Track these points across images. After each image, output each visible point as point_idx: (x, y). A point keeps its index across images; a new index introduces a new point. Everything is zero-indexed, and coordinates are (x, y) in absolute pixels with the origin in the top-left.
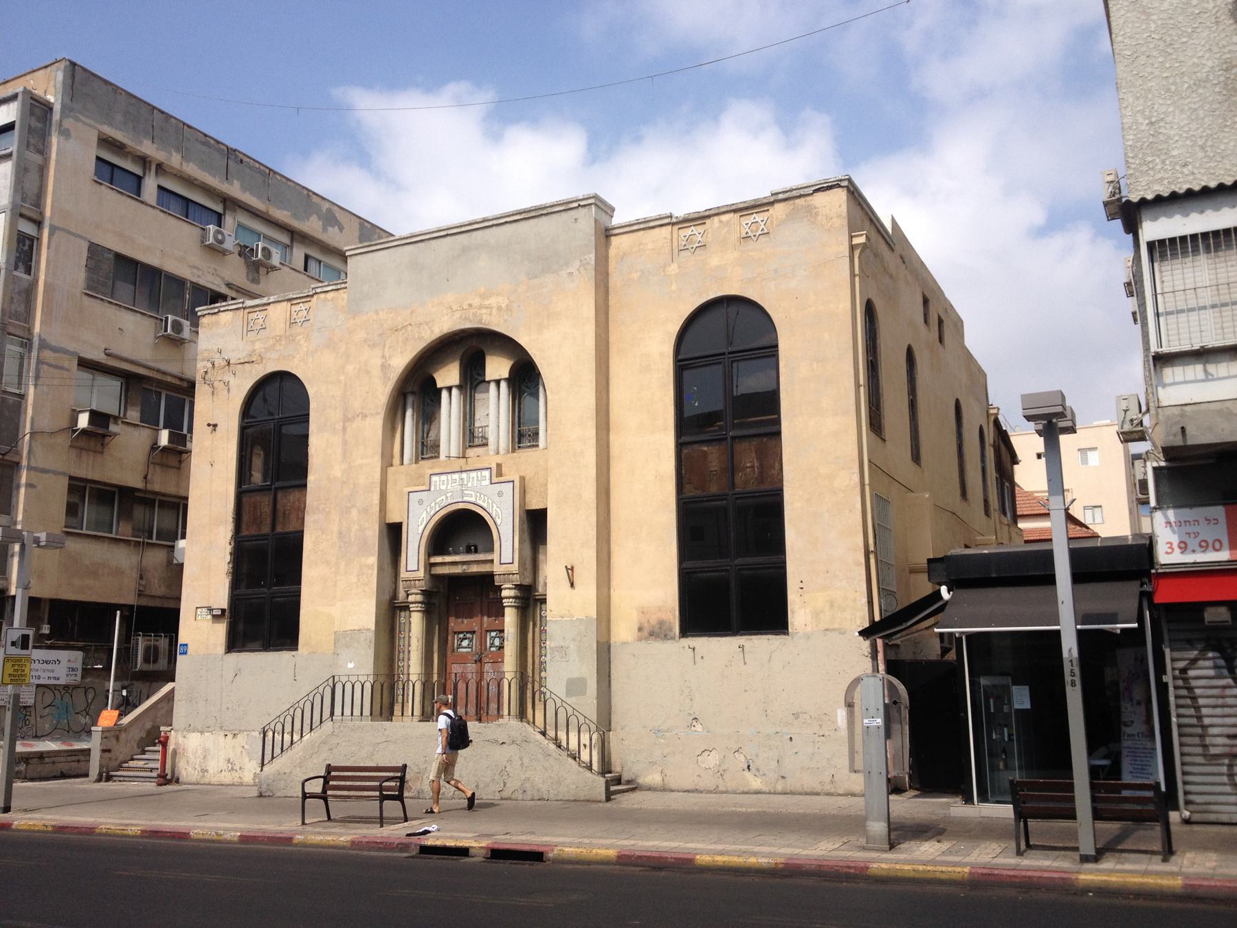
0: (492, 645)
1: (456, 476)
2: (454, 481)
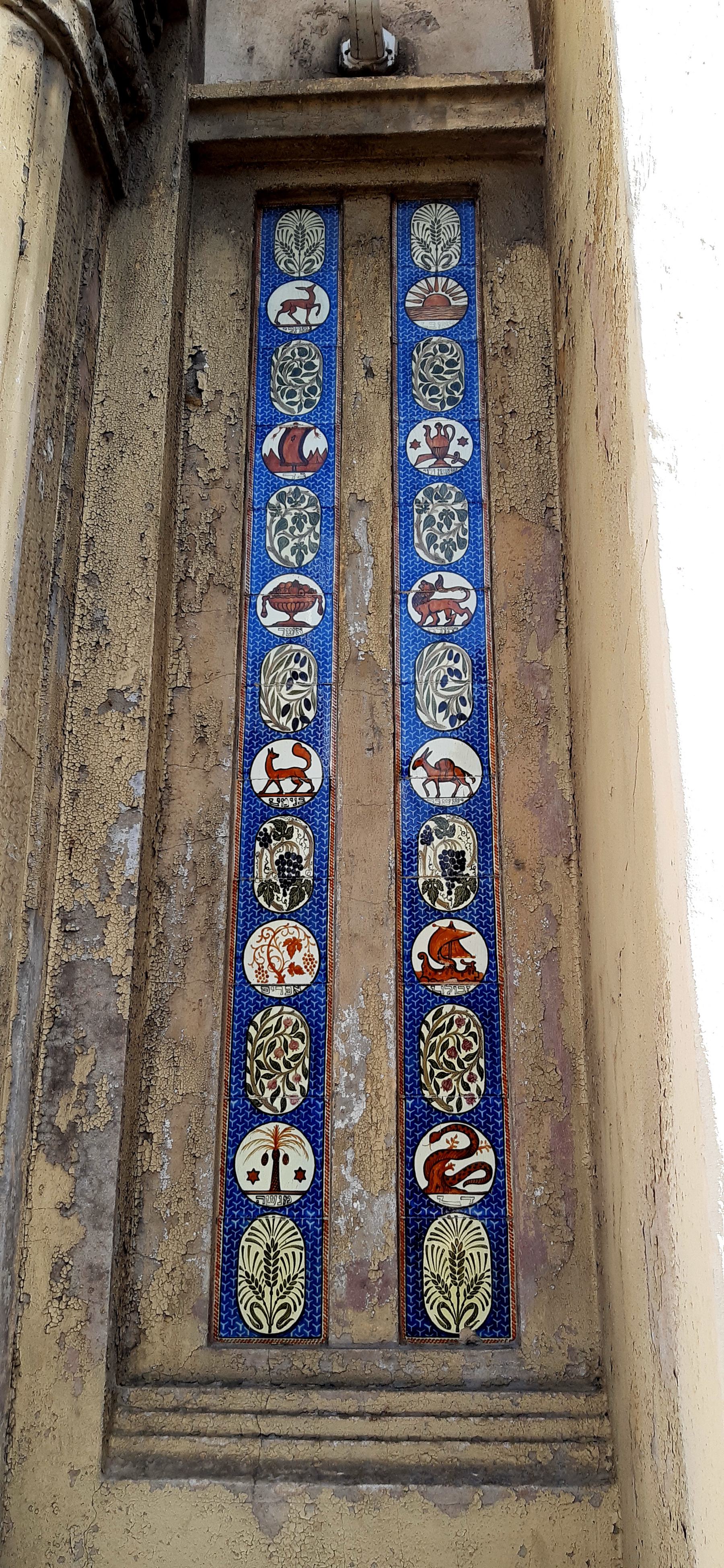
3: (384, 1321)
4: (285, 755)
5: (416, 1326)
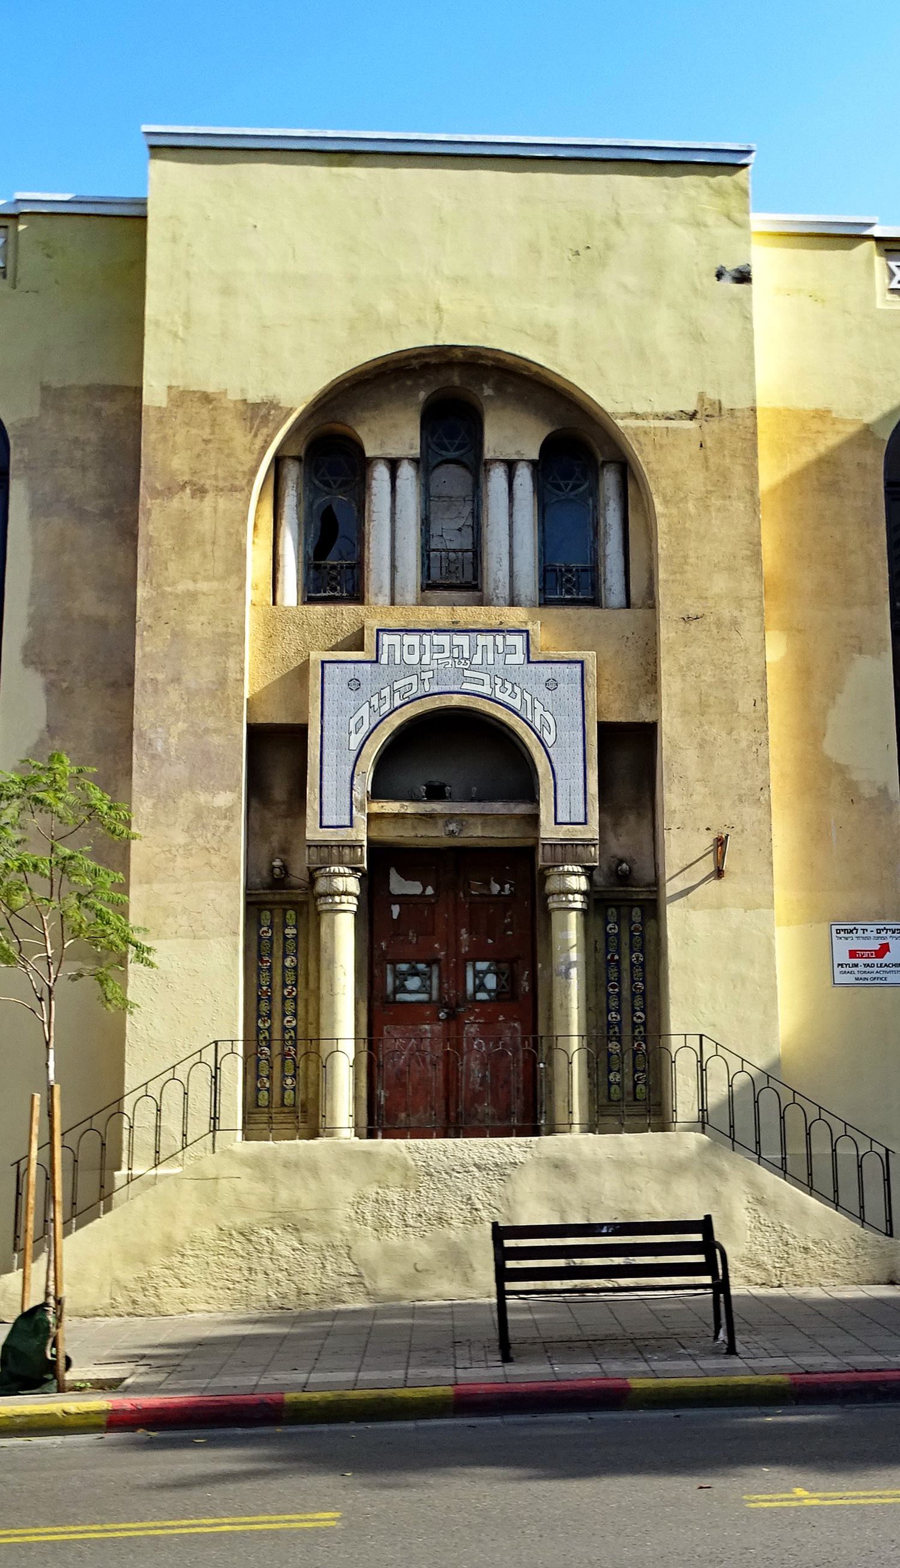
0: (480, 987)
1: (443, 639)
2: (441, 649)
3: (631, 1098)
4: (614, 1014)
5: (635, 1099)
